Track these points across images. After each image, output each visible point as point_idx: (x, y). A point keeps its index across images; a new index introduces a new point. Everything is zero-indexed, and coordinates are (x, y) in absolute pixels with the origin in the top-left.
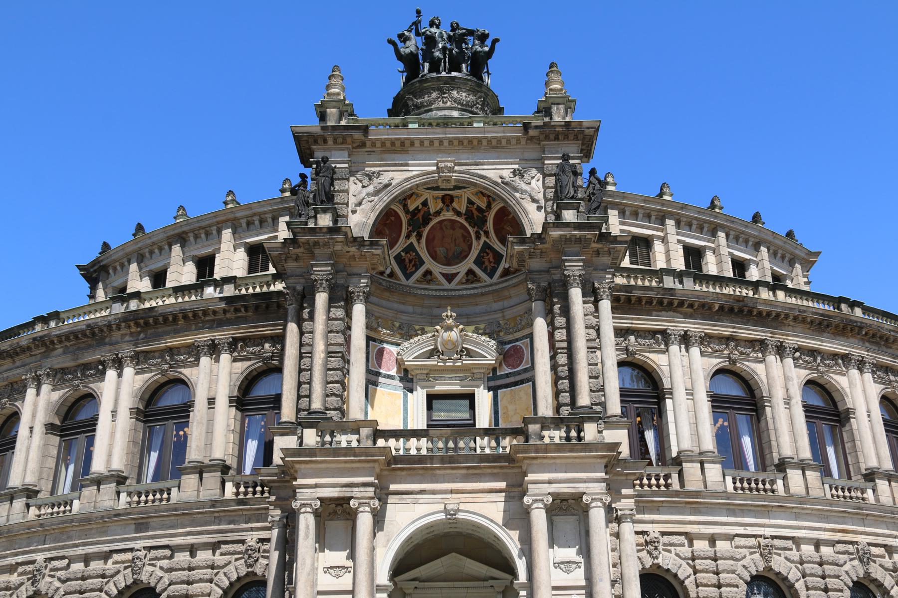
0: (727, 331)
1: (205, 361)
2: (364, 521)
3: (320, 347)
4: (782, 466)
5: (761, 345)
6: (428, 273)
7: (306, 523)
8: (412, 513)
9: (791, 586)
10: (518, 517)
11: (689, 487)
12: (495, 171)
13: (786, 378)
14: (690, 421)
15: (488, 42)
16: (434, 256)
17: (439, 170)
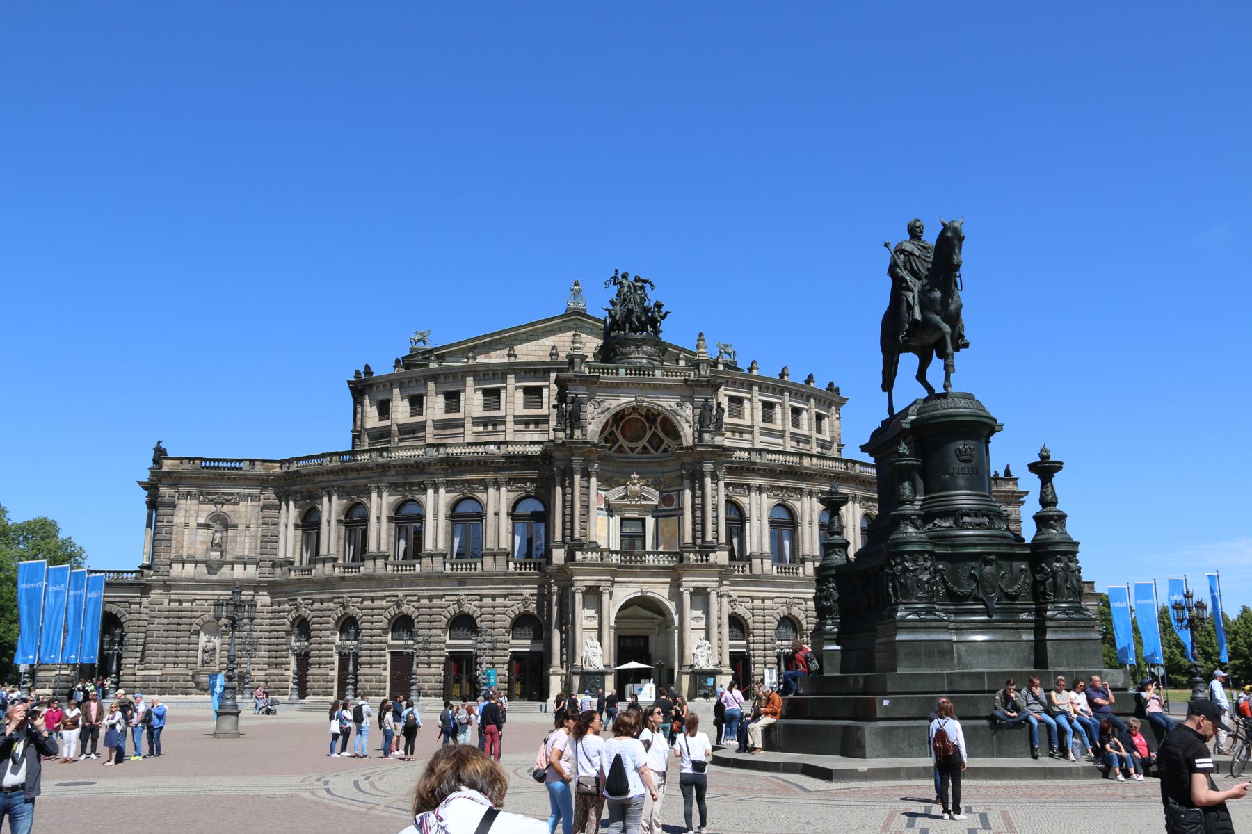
0: (782, 484)
1: (491, 490)
2: (606, 597)
3: (578, 505)
4: (803, 561)
5: (800, 491)
6: (621, 446)
7: (579, 597)
8: (624, 592)
9: (800, 622)
10: (676, 596)
11: (755, 572)
12: (667, 403)
13: (812, 510)
14: (758, 536)
15: (664, 310)
16: (624, 437)
17: (637, 401)
